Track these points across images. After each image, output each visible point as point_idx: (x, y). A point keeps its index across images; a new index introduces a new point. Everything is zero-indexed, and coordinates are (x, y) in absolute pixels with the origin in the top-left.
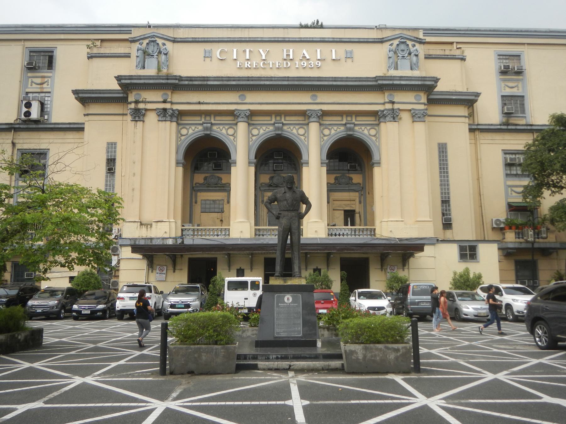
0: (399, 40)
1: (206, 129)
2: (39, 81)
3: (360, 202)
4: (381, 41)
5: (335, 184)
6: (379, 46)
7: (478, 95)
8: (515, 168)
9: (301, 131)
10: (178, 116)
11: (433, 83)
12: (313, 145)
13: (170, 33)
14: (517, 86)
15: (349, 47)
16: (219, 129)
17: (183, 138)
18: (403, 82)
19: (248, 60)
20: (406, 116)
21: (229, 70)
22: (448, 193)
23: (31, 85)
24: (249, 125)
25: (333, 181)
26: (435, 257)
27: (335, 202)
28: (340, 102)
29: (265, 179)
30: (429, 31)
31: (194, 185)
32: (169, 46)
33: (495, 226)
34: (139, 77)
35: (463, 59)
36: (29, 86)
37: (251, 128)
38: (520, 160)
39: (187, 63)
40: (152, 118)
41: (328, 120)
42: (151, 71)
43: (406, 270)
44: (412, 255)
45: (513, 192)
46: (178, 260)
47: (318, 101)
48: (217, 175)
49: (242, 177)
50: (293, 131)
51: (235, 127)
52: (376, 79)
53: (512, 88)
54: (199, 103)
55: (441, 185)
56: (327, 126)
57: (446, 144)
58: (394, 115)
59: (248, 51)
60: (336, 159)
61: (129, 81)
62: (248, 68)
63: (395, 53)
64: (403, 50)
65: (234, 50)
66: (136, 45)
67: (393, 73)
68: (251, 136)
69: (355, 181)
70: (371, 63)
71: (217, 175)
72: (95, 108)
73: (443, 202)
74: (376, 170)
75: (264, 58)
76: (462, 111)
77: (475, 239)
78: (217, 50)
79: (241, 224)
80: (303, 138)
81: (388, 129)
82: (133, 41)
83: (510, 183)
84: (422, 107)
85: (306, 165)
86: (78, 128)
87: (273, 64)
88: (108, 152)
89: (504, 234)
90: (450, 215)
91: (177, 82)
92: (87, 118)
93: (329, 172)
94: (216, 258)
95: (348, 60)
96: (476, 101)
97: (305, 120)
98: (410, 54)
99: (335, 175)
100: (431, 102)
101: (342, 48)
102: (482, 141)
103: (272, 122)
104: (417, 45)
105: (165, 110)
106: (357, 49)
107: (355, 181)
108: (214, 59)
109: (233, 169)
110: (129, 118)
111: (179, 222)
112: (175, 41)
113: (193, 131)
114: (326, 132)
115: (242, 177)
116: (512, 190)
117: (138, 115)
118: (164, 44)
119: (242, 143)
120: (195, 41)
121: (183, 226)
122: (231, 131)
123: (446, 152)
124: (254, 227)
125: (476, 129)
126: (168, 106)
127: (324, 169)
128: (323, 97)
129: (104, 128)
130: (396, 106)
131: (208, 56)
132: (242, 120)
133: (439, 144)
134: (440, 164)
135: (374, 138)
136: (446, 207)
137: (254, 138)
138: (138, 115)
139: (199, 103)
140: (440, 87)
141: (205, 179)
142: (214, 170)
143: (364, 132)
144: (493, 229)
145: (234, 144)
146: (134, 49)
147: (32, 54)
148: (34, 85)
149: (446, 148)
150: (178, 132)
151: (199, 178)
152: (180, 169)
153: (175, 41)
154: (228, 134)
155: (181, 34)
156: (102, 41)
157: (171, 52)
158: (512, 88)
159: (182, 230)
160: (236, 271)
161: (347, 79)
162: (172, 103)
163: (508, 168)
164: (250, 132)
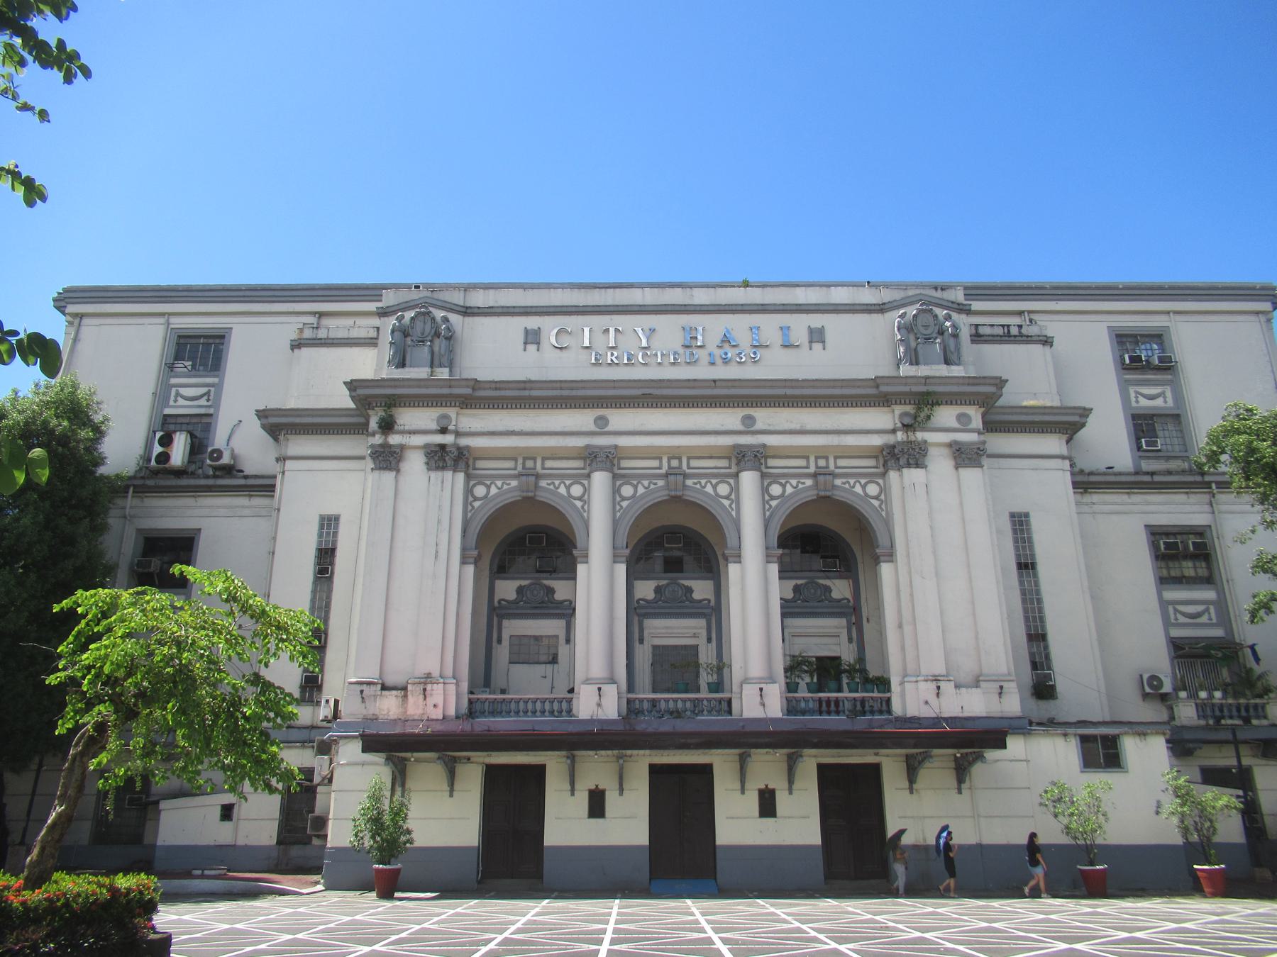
0: (918, 306)
3: (850, 640)
4: (881, 309)
5: (793, 600)
7: (1085, 412)
8: (1177, 565)
9: (723, 489)
11: (993, 389)
13: (457, 298)
14: (1162, 394)
15: (816, 320)
17: (477, 504)
19: (612, 348)
23: (176, 401)
25: (790, 595)
26: (1027, 761)
27: (797, 640)
29: (646, 589)
30: (976, 292)
31: (496, 604)
33: (1148, 690)
35: (1047, 341)
36: (172, 403)
37: (618, 483)
38: (1186, 547)
40: (415, 464)
44: (980, 757)
45: (1179, 616)
46: (461, 769)
47: (759, 425)
48: (546, 582)
49: (598, 585)
51: (585, 482)
52: (876, 382)
56: (775, 479)
57: (1027, 515)
59: (612, 331)
60: (795, 547)
62: (612, 364)
64: (926, 327)
65: (586, 329)
67: (906, 370)
68: (618, 499)
69: (835, 595)
71: (546, 582)
74: (886, 569)
75: (644, 344)
76: (1053, 444)
77: (1108, 719)
78: (550, 327)
80: (726, 503)
82: (383, 313)
83: (1172, 594)
84: (973, 437)
87: (662, 355)
88: (320, 535)
90: (1050, 668)
91: (468, 391)
93: (784, 573)
94: (544, 766)
95: (814, 345)
96: (1083, 425)
97: (729, 468)
99: (793, 582)
100: (991, 426)
103: (663, 471)
104: (955, 315)
105: (442, 447)
107: (835, 595)
109: (581, 568)
110: (370, 464)
111: (465, 686)
112: (467, 312)
113: (499, 489)
115: (598, 585)
116: (1176, 611)
118: (446, 320)
121: (472, 693)
124: (625, 696)
125: (1085, 483)
126: (448, 439)
127: (774, 568)
133: (1012, 515)
136: (1038, 646)
137: (625, 504)
138: (388, 459)
140: (1009, 397)
141: (520, 590)
142: (538, 571)
144: (1145, 696)
145: (582, 517)
147: (182, 341)
148: (181, 402)
149: (1028, 523)
150: (468, 491)
151: (507, 589)
152: (470, 569)
153: (467, 312)
159: (470, 702)
160: (586, 795)
162: (458, 434)
163: (1163, 564)
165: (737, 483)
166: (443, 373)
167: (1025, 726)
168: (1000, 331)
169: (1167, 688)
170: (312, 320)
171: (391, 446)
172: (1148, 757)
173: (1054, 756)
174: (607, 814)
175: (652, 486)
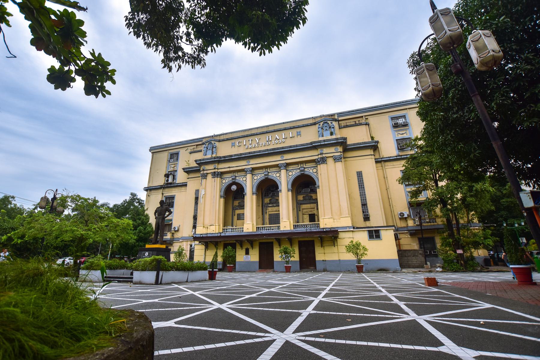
1: (233, 179)
2: (173, 166)
4: (315, 124)
6: (314, 126)
9: (278, 175)
10: (221, 175)
12: (284, 180)
13: (218, 138)
15: (298, 130)
18: (326, 143)
20: (330, 161)
21: (242, 150)
22: (366, 200)
24: (253, 175)
30: (340, 114)
32: (217, 144)
34: (203, 160)
35: (367, 124)
39: (224, 150)
40: (210, 177)
41: (291, 168)
42: (209, 156)
43: (336, 247)
50: (273, 175)
52: (311, 143)
53: (403, 134)
54: (229, 167)
55: (361, 195)
57: (361, 172)
58: (323, 160)
63: (322, 128)
64: (326, 127)
66: (204, 146)
67: (321, 139)
70: (310, 136)
72: (192, 175)
73: (366, 204)
76: (370, 152)
77: (385, 225)
78: (237, 142)
79: (249, 224)
81: (322, 168)
82: (203, 144)
84: (339, 154)
86: (184, 185)
89: (407, 221)
90: (368, 212)
92: (188, 180)
98: (330, 127)
101: (295, 131)
102: (386, 167)
105: (215, 172)
106: (302, 130)
108: (236, 146)
110: (200, 178)
112: (219, 141)
113: (228, 180)
114: (290, 174)
117: (205, 176)
119: (249, 184)
120: (228, 140)
122: (244, 179)
123: (362, 176)
126: (216, 170)
128: (287, 156)
129: (193, 184)
130: (324, 155)
131: (233, 145)
133: (357, 172)
134: (359, 184)
135: (316, 174)
139: (229, 167)
141: (239, 203)
143: (310, 171)
146: (202, 148)
155: (222, 138)
156: (197, 145)
157: (218, 146)
158: (403, 134)
161: (297, 146)
162: (218, 169)
164: (253, 178)
166: (214, 155)
167: (355, 228)
168: (354, 123)
169: (406, 216)
170: (195, 147)
172: (388, 235)
173: (362, 237)
174: (250, 253)
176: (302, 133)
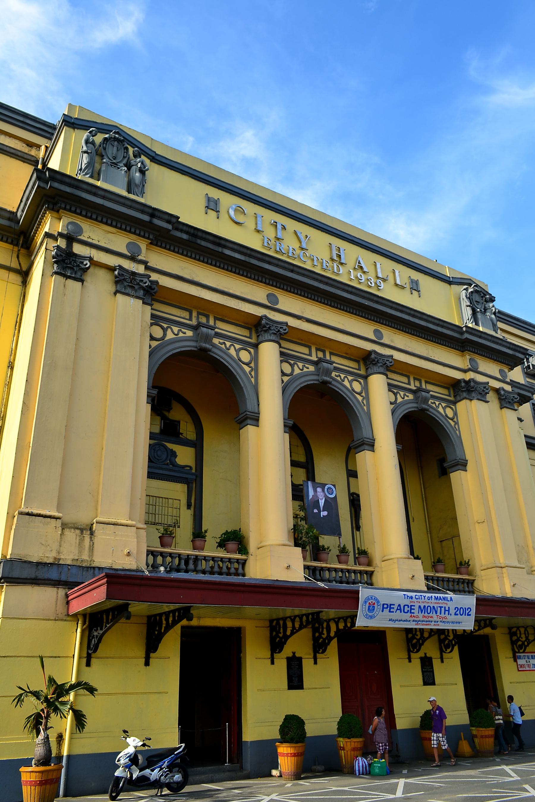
16: (223, 346)
28: (410, 350)
40: (100, 284)
47: (385, 340)
61: (68, 190)
78: (227, 201)
85: (370, 448)
91: (170, 227)
132: (273, 337)
154: (240, 360)
160: (285, 661)
165: (366, 384)
171: (76, 255)
175: (305, 370)
176: (422, 287)
